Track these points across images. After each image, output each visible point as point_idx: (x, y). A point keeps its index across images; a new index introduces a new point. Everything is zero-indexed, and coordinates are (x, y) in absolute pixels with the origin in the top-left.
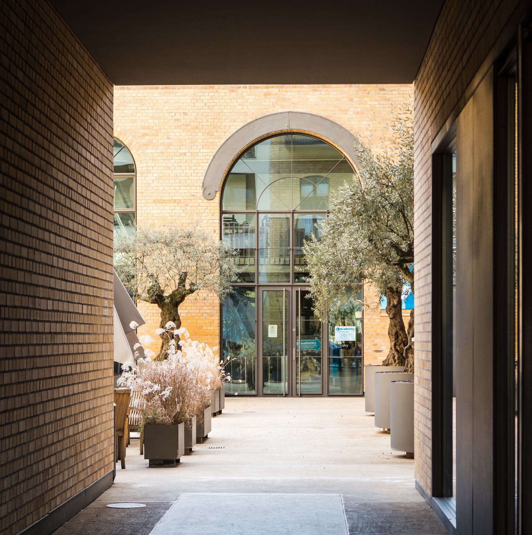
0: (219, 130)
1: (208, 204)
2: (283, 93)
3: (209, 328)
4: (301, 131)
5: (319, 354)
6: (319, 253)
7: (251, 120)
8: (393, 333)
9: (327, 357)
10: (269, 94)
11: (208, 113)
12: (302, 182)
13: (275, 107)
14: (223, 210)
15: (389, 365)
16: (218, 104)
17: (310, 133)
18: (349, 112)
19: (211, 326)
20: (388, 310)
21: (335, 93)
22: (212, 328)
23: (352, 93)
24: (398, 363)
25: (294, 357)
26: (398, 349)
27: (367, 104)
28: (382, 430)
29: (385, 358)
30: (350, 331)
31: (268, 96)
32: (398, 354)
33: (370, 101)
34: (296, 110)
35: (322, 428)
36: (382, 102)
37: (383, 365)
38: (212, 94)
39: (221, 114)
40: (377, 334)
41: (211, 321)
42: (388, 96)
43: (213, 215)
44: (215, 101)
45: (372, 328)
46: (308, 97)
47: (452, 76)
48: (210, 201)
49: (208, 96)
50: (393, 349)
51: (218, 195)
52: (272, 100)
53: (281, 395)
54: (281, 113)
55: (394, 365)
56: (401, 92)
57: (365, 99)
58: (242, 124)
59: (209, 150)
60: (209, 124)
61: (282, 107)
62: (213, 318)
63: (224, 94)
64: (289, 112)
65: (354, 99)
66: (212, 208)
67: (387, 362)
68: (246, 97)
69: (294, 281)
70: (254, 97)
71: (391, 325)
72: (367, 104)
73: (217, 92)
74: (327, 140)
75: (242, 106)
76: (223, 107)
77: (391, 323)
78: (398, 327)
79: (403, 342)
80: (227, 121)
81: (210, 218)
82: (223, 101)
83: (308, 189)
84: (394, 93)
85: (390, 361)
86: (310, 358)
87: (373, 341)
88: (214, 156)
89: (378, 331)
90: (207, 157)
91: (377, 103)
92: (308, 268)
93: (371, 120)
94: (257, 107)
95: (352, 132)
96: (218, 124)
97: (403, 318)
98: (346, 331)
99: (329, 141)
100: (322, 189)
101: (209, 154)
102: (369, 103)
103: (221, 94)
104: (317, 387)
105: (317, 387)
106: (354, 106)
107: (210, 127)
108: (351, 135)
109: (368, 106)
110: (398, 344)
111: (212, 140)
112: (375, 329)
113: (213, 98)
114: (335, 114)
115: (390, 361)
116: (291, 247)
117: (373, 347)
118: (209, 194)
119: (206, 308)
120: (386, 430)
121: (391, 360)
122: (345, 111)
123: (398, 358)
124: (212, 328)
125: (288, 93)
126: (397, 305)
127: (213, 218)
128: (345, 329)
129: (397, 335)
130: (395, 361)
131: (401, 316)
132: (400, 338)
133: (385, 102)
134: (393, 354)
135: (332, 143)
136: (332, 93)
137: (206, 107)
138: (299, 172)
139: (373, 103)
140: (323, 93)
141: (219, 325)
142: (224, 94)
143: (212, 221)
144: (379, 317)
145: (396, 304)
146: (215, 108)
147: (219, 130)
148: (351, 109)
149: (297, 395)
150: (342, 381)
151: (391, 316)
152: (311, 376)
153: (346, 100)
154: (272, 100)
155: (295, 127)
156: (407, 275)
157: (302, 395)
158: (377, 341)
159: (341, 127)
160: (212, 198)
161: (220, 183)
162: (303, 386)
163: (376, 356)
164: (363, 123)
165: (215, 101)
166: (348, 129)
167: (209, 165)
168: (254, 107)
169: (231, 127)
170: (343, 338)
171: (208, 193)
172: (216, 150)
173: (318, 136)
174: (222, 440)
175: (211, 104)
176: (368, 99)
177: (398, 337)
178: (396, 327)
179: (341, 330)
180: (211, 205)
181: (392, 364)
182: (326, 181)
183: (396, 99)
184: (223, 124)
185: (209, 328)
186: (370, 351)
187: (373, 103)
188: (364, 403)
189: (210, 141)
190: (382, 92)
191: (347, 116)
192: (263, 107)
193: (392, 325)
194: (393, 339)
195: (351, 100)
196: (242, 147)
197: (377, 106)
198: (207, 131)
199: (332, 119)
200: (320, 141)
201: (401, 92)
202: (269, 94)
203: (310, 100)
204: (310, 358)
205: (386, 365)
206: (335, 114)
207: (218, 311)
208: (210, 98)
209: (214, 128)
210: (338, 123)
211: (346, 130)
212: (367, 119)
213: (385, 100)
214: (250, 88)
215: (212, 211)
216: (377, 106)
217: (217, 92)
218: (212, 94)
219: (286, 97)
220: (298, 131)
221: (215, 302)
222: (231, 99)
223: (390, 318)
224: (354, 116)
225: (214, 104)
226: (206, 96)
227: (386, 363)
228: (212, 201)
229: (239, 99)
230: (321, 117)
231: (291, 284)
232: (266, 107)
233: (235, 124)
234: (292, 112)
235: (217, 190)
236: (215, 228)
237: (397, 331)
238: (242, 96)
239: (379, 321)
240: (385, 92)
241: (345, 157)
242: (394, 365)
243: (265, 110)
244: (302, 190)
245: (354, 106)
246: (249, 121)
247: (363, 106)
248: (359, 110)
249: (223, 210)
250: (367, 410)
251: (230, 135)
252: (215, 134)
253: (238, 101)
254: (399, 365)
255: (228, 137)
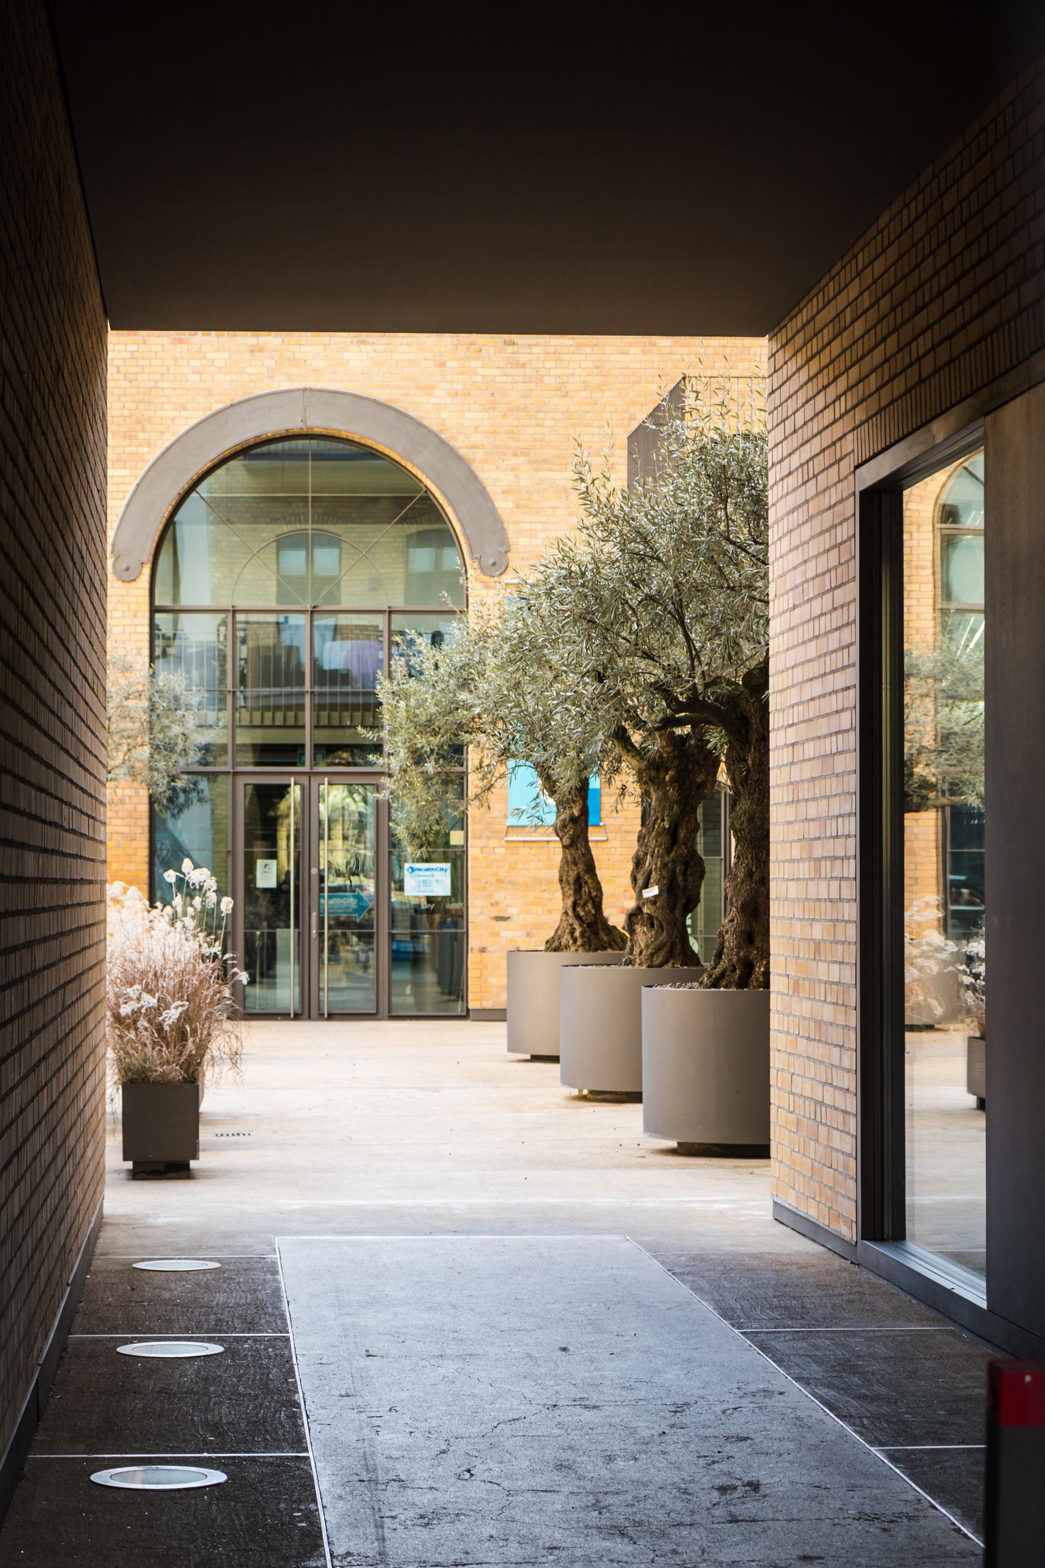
0: (149, 427)
1: (123, 592)
2: (292, 348)
3: (126, 867)
4: (330, 432)
5: (367, 924)
6: (412, 702)
7: (220, 406)
8: (571, 879)
9: (386, 931)
10: (261, 350)
11: (125, 388)
12: (282, 544)
13: (272, 377)
14: (157, 604)
15: (561, 950)
16: (147, 370)
17: (350, 436)
18: (437, 392)
19: (129, 862)
20: (560, 830)
21: (406, 349)
22: (132, 867)
23: (443, 349)
24: (582, 945)
25: (314, 932)
26: (582, 914)
27: (476, 374)
28: (575, 1092)
29: (552, 934)
30: (438, 875)
31: (257, 354)
32: (581, 926)
33: (483, 367)
34: (319, 386)
35: (437, 1090)
36: (509, 371)
37: (547, 950)
38: (134, 348)
39: (153, 392)
40: (500, 881)
41: (130, 851)
42: (523, 358)
43: (135, 616)
44: (140, 362)
45: (488, 866)
46: (346, 356)
47: (42, 307)
48: (128, 585)
49: (125, 351)
50: (570, 913)
51: (146, 571)
52: (267, 363)
53: (284, 1016)
54: (287, 391)
55: (573, 948)
56: (552, 350)
57: (473, 364)
58: (201, 415)
59: (127, 472)
60: (126, 413)
61: (290, 378)
62: (135, 844)
63: (159, 348)
64: (305, 390)
65: (449, 364)
66: (133, 600)
67: (556, 944)
68: (210, 356)
69: (315, 763)
70: (226, 355)
71: (565, 862)
72: (476, 374)
73: (145, 342)
74: (387, 451)
75: (200, 374)
76: (157, 377)
77: (565, 858)
78: (581, 866)
79: (591, 898)
80: (166, 406)
81: (128, 621)
82: (159, 362)
83: (295, 560)
84: (535, 350)
85: (564, 941)
86: (344, 935)
87: (490, 896)
88: (138, 485)
89: (502, 874)
90: (122, 488)
91: (498, 372)
92: (382, 734)
93: (485, 410)
94: (234, 377)
95: (443, 436)
96: (148, 414)
97: (591, 845)
98: (428, 873)
99: (392, 455)
100: (326, 559)
101: (127, 480)
102: (480, 371)
103: (154, 348)
104: (360, 998)
105: (360, 998)
106: (448, 378)
107: (128, 420)
108: (442, 442)
109: (479, 379)
110: (581, 902)
111: (134, 450)
112: (494, 870)
113: (136, 355)
114: (406, 394)
115: (564, 941)
116: (307, 687)
117: (491, 908)
118: (127, 569)
119: (119, 822)
120: (585, 1092)
121: (566, 939)
122: (429, 389)
123: (582, 934)
124: (132, 867)
125: (303, 348)
126: (579, 817)
127: (135, 621)
128: (427, 870)
129: (578, 884)
130: (575, 941)
131: (587, 841)
132: (585, 889)
133: (516, 371)
134: (571, 925)
135: (398, 459)
136: (401, 349)
137: (121, 376)
138: (275, 521)
139: (489, 372)
140: (380, 348)
141: (146, 860)
142: (159, 348)
143: (132, 629)
144: (505, 844)
145: (576, 814)
146: (139, 378)
147: (149, 427)
148: (442, 385)
149: (321, 1017)
150: (417, 985)
151: (566, 841)
152: (347, 974)
153: (431, 364)
154: (267, 363)
155: (318, 423)
156: (628, 751)
157: (331, 1017)
158: (499, 896)
159: (420, 425)
160: (132, 578)
161: (151, 545)
162: (337, 997)
163: (497, 928)
164: (468, 415)
165: (140, 362)
166: (435, 428)
167: (128, 505)
168: (228, 377)
169: (177, 422)
170: (423, 889)
171: (124, 566)
172: (142, 473)
173: (369, 443)
174: (234, 1118)
175: (132, 370)
176: (479, 363)
177: (580, 887)
178: (576, 865)
179: (417, 872)
180: (132, 592)
181: (567, 947)
182: (334, 542)
183: (540, 365)
184: (159, 413)
185: (126, 867)
186: (484, 918)
187: (489, 372)
188: (505, 1032)
189: (128, 450)
190: (510, 349)
191: (433, 400)
192: (246, 378)
193: (567, 862)
194: (571, 892)
195: (442, 365)
196: (201, 466)
197: (497, 379)
198: (123, 429)
199: (399, 406)
200: (370, 453)
201: (552, 350)
202: (261, 350)
203: (352, 364)
204: (344, 935)
205: (556, 950)
206: (406, 394)
207: (147, 829)
208: (128, 355)
209: (139, 422)
210: (413, 414)
211: (430, 431)
212: (475, 407)
213: (517, 365)
214: (217, 336)
215: (133, 607)
216: (497, 379)
217: (145, 342)
218: (134, 348)
219: (298, 355)
220: (324, 432)
221: (139, 808)
222: (175, 359)
223: (564, 847)
224: (449, 400)
225: (138, 369)
226: (119, 351)
227: (554, 946)
228: (133, 584)
229: (193, 358)
230: (375, 402)
231: (306, 769)
232: (253, 378)
233: (184, 413)
234: (311, 390)
235: (145, 560)
236: (139, 645)
237: (578, 874)
238: (199, 352)
239: (502, 851)
240: (515, 348)
241: (428, 490)
242: (573, 948)
243: (252, 385)
244: (281, 559)
245: (448, 378)
246: (216, 407)
247: (467, 378)
248: (459, 387)
249: (157, 604)
250: (511, 1049)
251: (173, 439)
252: (141, 435)
253: (193, 363)
254: (585, 950)
255: (168, 444)
